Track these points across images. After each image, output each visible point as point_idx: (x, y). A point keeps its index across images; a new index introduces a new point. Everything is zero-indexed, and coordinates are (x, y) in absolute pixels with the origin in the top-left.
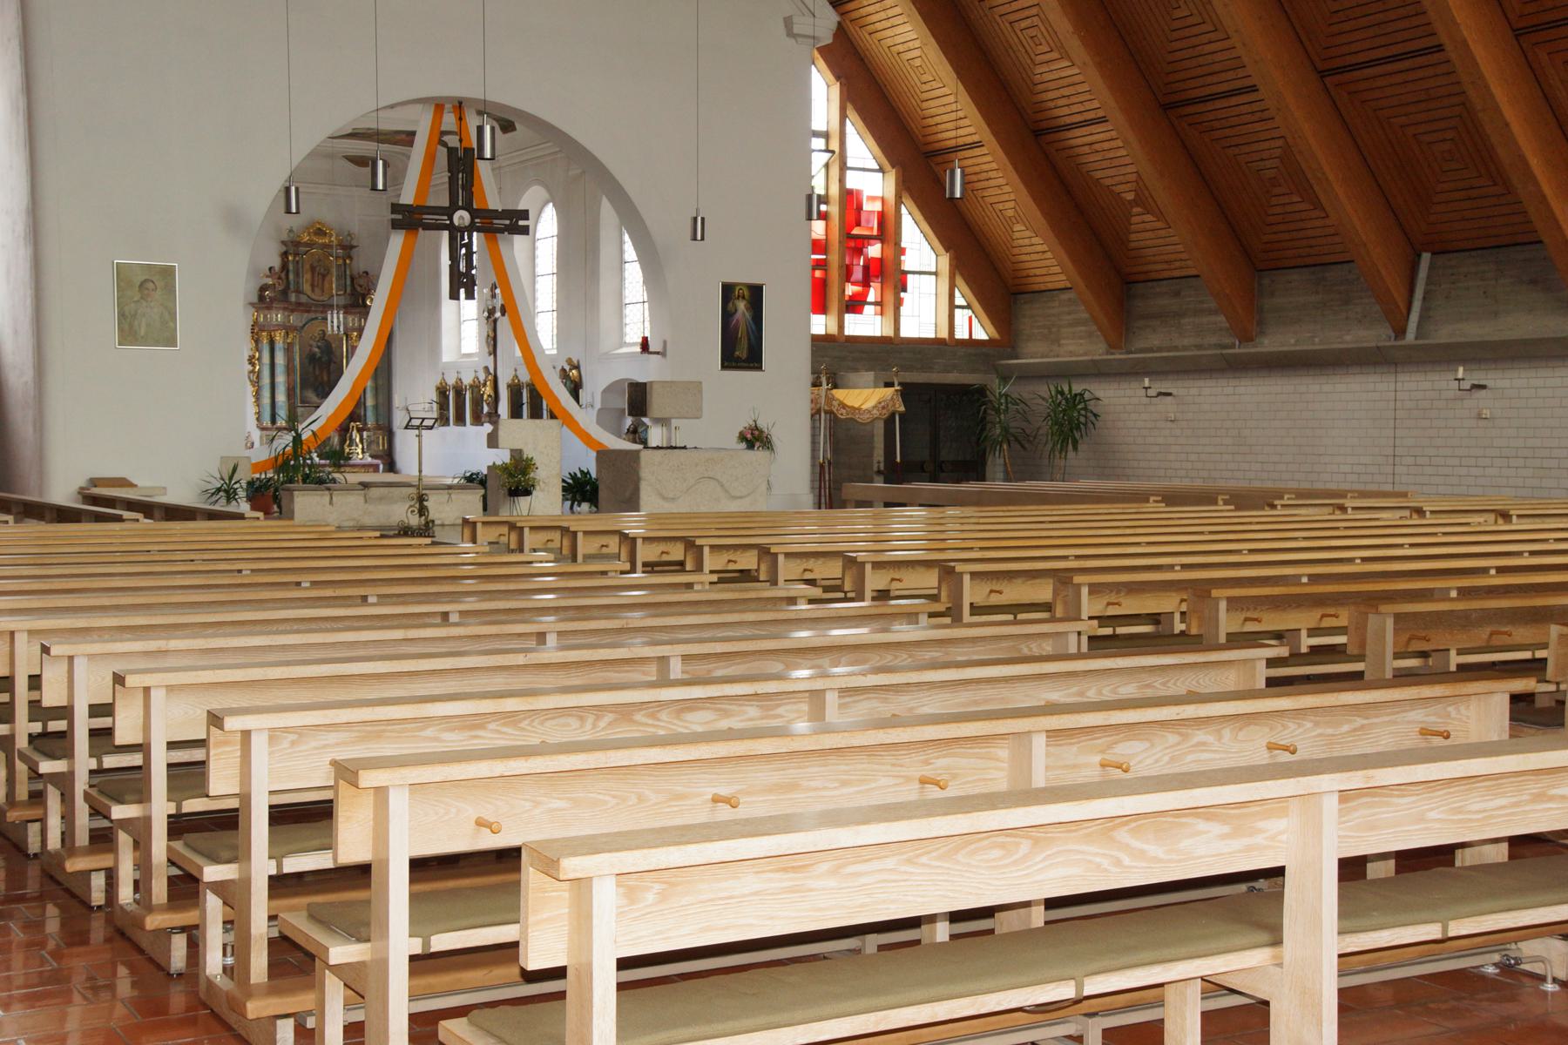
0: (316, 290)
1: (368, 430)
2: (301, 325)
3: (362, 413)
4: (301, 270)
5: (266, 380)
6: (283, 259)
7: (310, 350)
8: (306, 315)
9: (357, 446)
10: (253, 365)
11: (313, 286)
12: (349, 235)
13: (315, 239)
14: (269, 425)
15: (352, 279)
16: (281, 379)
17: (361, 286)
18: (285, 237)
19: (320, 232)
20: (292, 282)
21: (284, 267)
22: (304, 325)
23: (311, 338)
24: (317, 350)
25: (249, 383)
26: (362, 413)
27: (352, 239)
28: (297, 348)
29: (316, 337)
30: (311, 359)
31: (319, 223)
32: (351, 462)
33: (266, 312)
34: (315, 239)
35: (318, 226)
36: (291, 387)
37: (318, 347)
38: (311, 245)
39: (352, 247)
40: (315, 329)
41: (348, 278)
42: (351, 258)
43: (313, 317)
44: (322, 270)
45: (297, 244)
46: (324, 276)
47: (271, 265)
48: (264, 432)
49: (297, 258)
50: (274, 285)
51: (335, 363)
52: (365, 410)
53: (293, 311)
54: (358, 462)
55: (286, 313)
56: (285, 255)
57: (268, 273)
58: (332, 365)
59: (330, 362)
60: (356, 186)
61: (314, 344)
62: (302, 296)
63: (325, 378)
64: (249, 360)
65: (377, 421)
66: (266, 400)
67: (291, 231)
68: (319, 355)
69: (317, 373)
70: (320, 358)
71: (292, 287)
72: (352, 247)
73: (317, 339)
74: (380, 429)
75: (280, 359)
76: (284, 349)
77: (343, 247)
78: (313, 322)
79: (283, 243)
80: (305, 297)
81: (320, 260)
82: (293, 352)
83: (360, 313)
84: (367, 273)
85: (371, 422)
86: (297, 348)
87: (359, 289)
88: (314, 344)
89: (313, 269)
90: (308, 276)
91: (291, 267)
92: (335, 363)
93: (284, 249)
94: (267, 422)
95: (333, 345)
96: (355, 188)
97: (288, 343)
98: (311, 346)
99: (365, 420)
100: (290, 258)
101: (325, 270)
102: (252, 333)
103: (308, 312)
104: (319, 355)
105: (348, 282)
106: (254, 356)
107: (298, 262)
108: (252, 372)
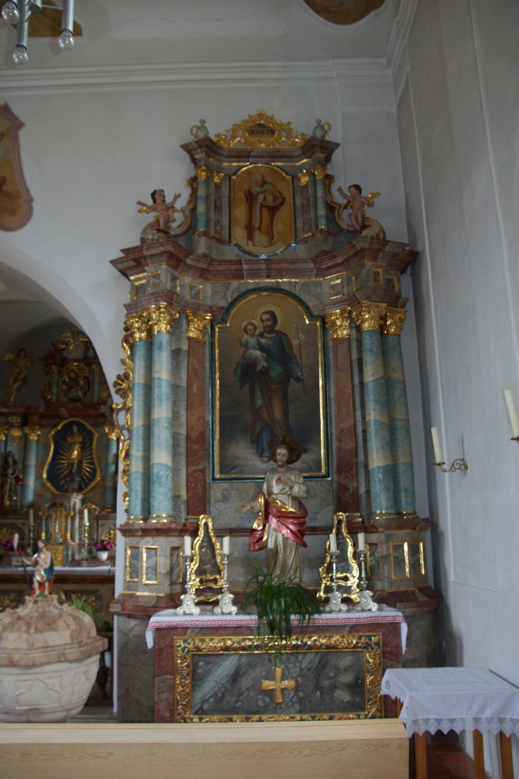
0: (257, 235)
2: (224, 303)
3: (362, 490)
7: (245, 352)
8: (235, 284)
22: (232, 304)
23: (245, 330)
24: (258, 353)
29: (255, 328)
36: (194, 435)
37: (261, 348)
41: (322, 211)
44: (270, 200)
46: (273, 210)
51: (298, 380)
52: (368, 481)
61: (252, 341)
65: (396, 502)
68: (262, 364)
69: (259, 402)
70: (265, 371)
73: (257, 332)
74: (401, 526)
81: (264, 183)
88: (252, 341)
92: (298, 380)
97: (189, 339)
98: (246, 346)
99: (369, 504)
101: (275, 198)
104: (262, 364)
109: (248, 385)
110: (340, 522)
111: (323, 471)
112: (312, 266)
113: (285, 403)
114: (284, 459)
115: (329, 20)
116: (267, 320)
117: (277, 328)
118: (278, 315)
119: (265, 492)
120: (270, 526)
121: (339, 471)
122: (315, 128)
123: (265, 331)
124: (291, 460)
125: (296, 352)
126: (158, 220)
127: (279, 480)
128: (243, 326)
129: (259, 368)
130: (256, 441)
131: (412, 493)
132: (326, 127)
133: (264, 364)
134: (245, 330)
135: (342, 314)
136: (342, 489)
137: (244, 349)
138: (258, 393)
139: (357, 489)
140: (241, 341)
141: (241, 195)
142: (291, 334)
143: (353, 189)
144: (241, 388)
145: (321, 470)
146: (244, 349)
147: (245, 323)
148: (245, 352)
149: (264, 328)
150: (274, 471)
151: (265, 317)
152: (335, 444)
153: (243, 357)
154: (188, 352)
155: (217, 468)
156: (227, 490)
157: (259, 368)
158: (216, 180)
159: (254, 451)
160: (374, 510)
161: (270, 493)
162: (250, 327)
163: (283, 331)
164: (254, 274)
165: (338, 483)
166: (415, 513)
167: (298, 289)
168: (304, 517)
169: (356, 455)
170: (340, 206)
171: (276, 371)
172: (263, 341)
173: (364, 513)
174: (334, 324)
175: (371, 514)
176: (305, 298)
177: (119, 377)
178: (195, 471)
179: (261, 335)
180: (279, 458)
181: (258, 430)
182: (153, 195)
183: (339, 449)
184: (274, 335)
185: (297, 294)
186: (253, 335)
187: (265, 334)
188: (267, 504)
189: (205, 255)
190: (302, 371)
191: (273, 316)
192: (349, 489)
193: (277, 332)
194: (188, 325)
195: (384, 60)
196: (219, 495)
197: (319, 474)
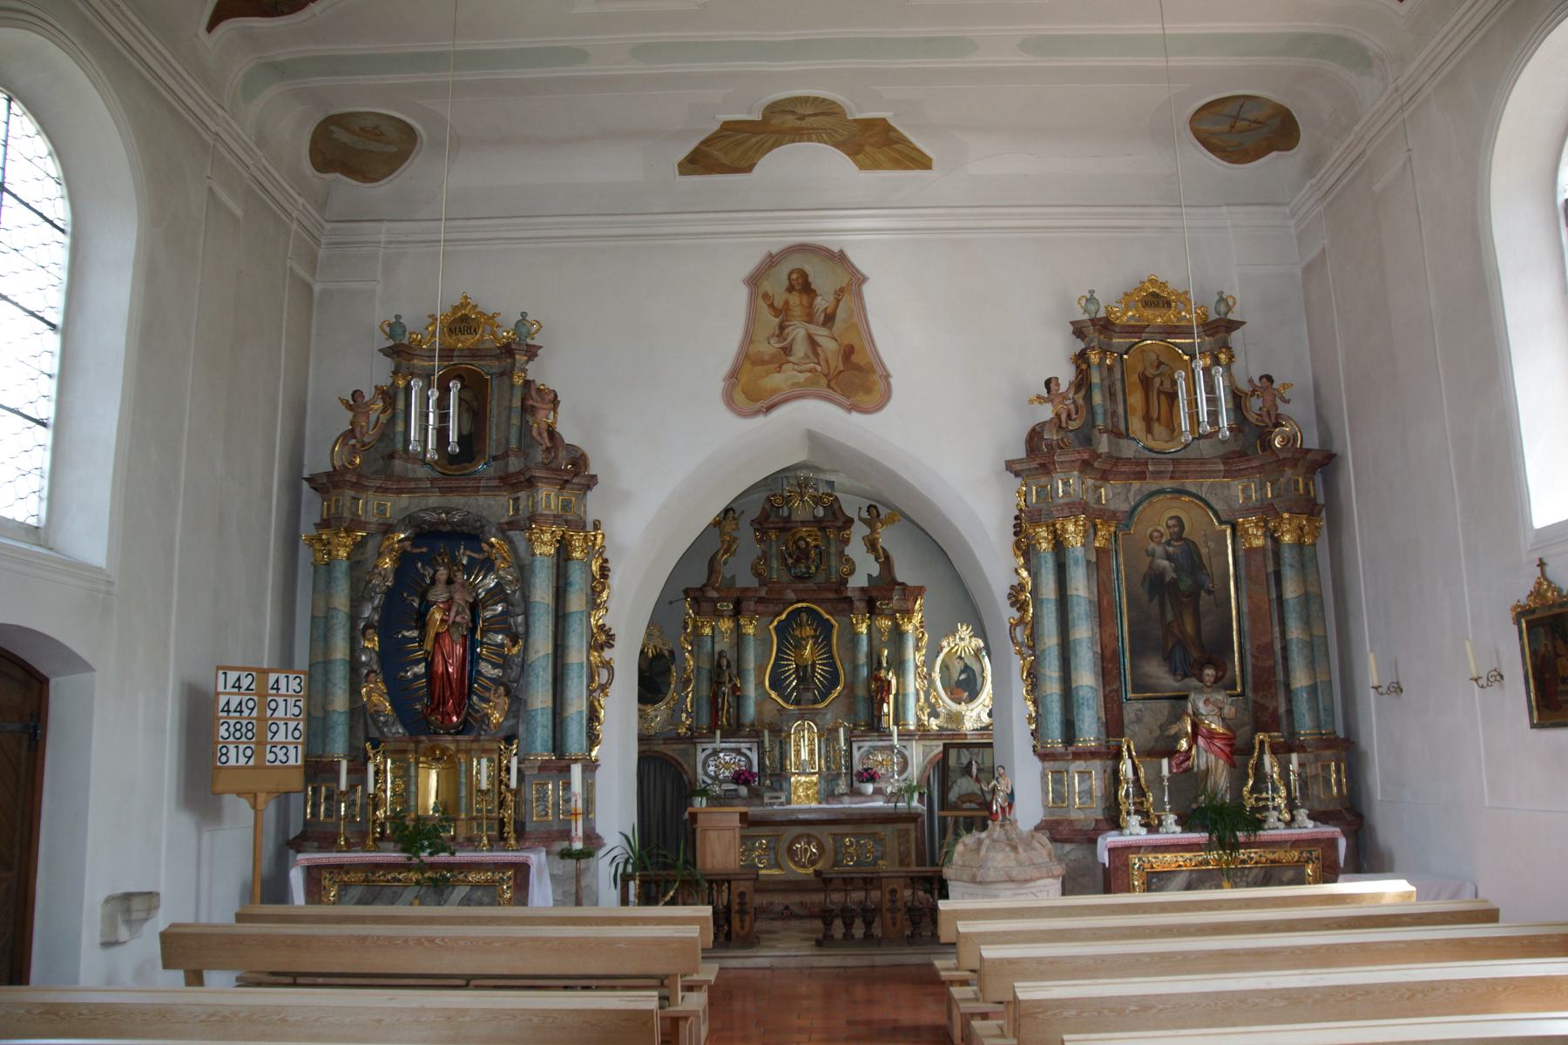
0: (1157, 427)
1: (1301, 749)
2: (1125, 507)
3: (1282, 709)
4: (1118, 386)
5: (1050, 640)
6: (1078, 367)
7: (1152, 562)
8: (1136, 485)
9: (1275, 790)
10: (1021, 606)
11: (1148, 420)
16: (1083, 632)
19: (1156, 299)
20: (1099, 411)
21: (1082, 382)
23: (1151, 537)
24: (1165, 563)
25: (1013, 649)
26: (1282, 709)
27: (1229, 309)
28: (1119, 564)
30: (1156, 583)
31: (1153, 282)
32: (1264, 835)
33: (1044, 480)
36: (1108, 652)
37: (1169, 557)
39: (1233, 326)
40: (1159, 517)
43: (1154, 487)
45: (1105, 326)
48: (1050, 765)
51: (1209, 592)
52: (1289, 701)
53: (1104, 476)
54: (1282, 832)
55: (1090, 482)
56: (1081, 358)
57: (1044, 392)
59: (1197, 589)
60: (1228, 205)
61: (1159, 550)
62: (1123, 442)
63: (1189, 628)
66: (1052, 688)
67: (1091, 299)
69: (1170, 616)
70: (1174, 583)
71: (1100, 422)
72: (1233, 326)
73: (1164, 540)
74: (1328, 747)
75: (1080, 586)
76: (1088, 562)
78: (1155, 499)
79: (1079, 331)
81: (1160, 364)
82: (1110, 571)
83: (1261, 469)
84: (1269, 379)
85: (1305, 727)
86: (1119, 564)
88: (1159, 550)
89: (1146, 382)
90: (1136, 399)
91: (1095, 378)
92: (1209, 592)
93: (1080, 345)
95: (1204, 551)
96: (1224, 210)
97: (1097, 549)
98: (1152, 554)
100: (1094, 358)
102: (1016, 534)
103: (1141, 476)
108: (1021, 621)
109: (1157, 598)
110: (1262, 743)
112: (1222, 467)
114: (1212, 679)
115: (1223, 158)
116: (1174, 526)
117: (1184, 535)
118: (1184, 521)
119: (1190, 711)
120: (1198, 747)
121: (1255, 690)
122: (1218, 302)
123: (1172, 539)
124: (1217, 680)
125: (1205, 562)
126: (1058, 416)
127: (1206, 702)
128: (1148, 533)
129: (1168, 579)
130: (1168, 659)
131: (1330, 711)
132: (1230, 302)
133: (1174, 576)
134: (1151, 537)
136: (1259, 708)
137: (1150, 558)
138: (1169, 607)
139: (1276, 709)
140: (1147, 551)
141: (1134, 378)
142: (1199, 541)
143: (1264, 380)
144: (1151, 600)
145: (1236, 689)
146: (1150, 558)
147: (1150, 530)
148: (1152, 562)
149: (1171, 535)
150: (1200, 691)
151: (1171, 523)
152: (1249, 661)
153: (1150, 567)
154: (1097, 563)
155: (1129, 688)
156: (1140, 710)
157: (1168, 579)
159: (1167, 669)
160: (1297, 730)
161: (1196, 714)
162: (1156, 534)
163: (1190, 537)
164: (1158, 475)
165: (1255, 702)
166: (1335, 733)
167: (1205, 489)
168: (1234, 738)
169: (1275, 675)
170: (1246, 394)
171: (1186, 584)
172: (1171, 549)
173: (1286, 734)
174: (1246, 531)
175: (1293, 734)
176: (1213, 501)
177: (1012, 587)
178: (1111, 692)
179: (1168, 543)
180: (1207, 678)
181: (1170, 645)
183: (1254, 667)
184: (1182, 542)
185: (1204, 496)
186: (1159, 543)
187: (1173, 542)
188: (1195, 726)
189: (1109, 456)
190: (1212, 582)
192: (1268, 709)
193: (1185, 539)
194: (1095, 534)
195: (1287, 210)
196: (1133, 715)
197: (1235, 692)
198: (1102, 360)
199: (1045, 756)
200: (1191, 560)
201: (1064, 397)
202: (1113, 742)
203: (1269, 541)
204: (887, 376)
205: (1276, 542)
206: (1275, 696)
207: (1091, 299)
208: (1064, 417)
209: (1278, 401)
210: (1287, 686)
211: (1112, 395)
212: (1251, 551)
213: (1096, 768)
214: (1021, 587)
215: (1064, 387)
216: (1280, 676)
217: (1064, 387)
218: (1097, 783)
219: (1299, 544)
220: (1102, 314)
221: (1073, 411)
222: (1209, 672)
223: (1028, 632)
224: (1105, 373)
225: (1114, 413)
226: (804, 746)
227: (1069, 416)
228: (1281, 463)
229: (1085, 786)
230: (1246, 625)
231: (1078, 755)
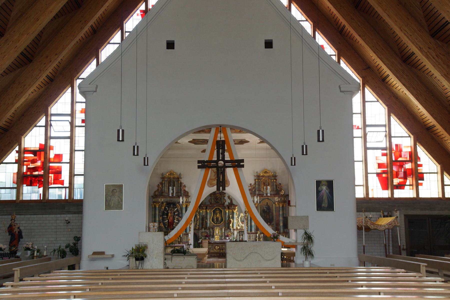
3: (279, 228)
4: (260, 184)
8: (262, 198)
12: (275, 172)
13: (264, 174)
14: (250, 232)
15: (276, 186)
17: (279, 188)
18: (256, 175)
19: (266, 172)
21: (255, 184)
23: (264, 205)
31: (266, 169)
34: (264, 174)
35: (266, 170)
37: (266, 208)
38: (263, 176)
42: (276, 180)
47: (250, 183)
49: (259, 181)
50: (251, 189)
51: (271, 212)
57: (250, 186)
58: (270, 213)
61: (264, 206)
63: (268, 217)
64: (245, 212)
66: (249, 225)
67: (257, 172)
73: (265, 205)
77: (273, 176)
79: (255, 176)
80: (262, 192)
83: (278, 196)
87: (278, 189)
88: (264, 206)
91: (257, 183)
92: (271, 212)
94: (249, 232)
95: (271, 207)
98: (264, 207)
99: (280, 230)
104: (266, 210)
105: (275, 187)
106: (246, 211)
107: (259, 182)
108: (246, 216)
111: (274, 225)
113: (269, 216)
125: (271, 208)
134: (264, 205)
135: (277, 204)
141: (263, 183)
142: (270, 206)
158: (259, 181)
171: (268, 211)
174: (276, 205)
175: (280, 232)
177: (245, 211)
182: (250, 184)
191: (267, 203)
193: (268, 205)
198: (258, 181)
199: (248, 233)
200: (269, 208)
201: (253, 186)
202: (257, 232)
203: (279, 206)
204: (229, 182)
205: (280, 206)
206: (279, 227)
207: (257, 172)
208: (252, 189)
209: (281, 187)
210: (280, 225)
211: (259, 185)
212: (276, 207)
213: (254, 235)
214: (246, 211)
215: (252, 185)
216: (279, 224)
217: (252, 185)
218: (254, 237)
219: (283, 206)
220: (258, 175)
221: (253, 188)
222: (269, 223)
223: (247, 217)
224: (258, 182)
225: (259, 188)
226: (217, 231)
227: (253, 189)
228: (280, 196)
229: (252, 237)
230: (276, 217)
231: (252, 233)
